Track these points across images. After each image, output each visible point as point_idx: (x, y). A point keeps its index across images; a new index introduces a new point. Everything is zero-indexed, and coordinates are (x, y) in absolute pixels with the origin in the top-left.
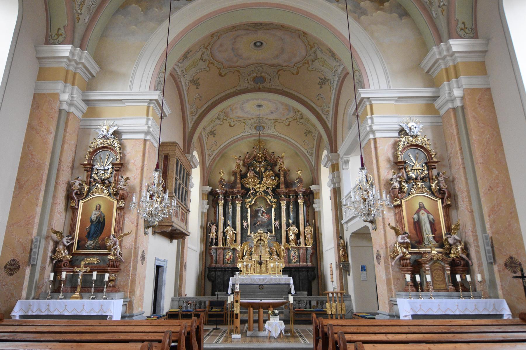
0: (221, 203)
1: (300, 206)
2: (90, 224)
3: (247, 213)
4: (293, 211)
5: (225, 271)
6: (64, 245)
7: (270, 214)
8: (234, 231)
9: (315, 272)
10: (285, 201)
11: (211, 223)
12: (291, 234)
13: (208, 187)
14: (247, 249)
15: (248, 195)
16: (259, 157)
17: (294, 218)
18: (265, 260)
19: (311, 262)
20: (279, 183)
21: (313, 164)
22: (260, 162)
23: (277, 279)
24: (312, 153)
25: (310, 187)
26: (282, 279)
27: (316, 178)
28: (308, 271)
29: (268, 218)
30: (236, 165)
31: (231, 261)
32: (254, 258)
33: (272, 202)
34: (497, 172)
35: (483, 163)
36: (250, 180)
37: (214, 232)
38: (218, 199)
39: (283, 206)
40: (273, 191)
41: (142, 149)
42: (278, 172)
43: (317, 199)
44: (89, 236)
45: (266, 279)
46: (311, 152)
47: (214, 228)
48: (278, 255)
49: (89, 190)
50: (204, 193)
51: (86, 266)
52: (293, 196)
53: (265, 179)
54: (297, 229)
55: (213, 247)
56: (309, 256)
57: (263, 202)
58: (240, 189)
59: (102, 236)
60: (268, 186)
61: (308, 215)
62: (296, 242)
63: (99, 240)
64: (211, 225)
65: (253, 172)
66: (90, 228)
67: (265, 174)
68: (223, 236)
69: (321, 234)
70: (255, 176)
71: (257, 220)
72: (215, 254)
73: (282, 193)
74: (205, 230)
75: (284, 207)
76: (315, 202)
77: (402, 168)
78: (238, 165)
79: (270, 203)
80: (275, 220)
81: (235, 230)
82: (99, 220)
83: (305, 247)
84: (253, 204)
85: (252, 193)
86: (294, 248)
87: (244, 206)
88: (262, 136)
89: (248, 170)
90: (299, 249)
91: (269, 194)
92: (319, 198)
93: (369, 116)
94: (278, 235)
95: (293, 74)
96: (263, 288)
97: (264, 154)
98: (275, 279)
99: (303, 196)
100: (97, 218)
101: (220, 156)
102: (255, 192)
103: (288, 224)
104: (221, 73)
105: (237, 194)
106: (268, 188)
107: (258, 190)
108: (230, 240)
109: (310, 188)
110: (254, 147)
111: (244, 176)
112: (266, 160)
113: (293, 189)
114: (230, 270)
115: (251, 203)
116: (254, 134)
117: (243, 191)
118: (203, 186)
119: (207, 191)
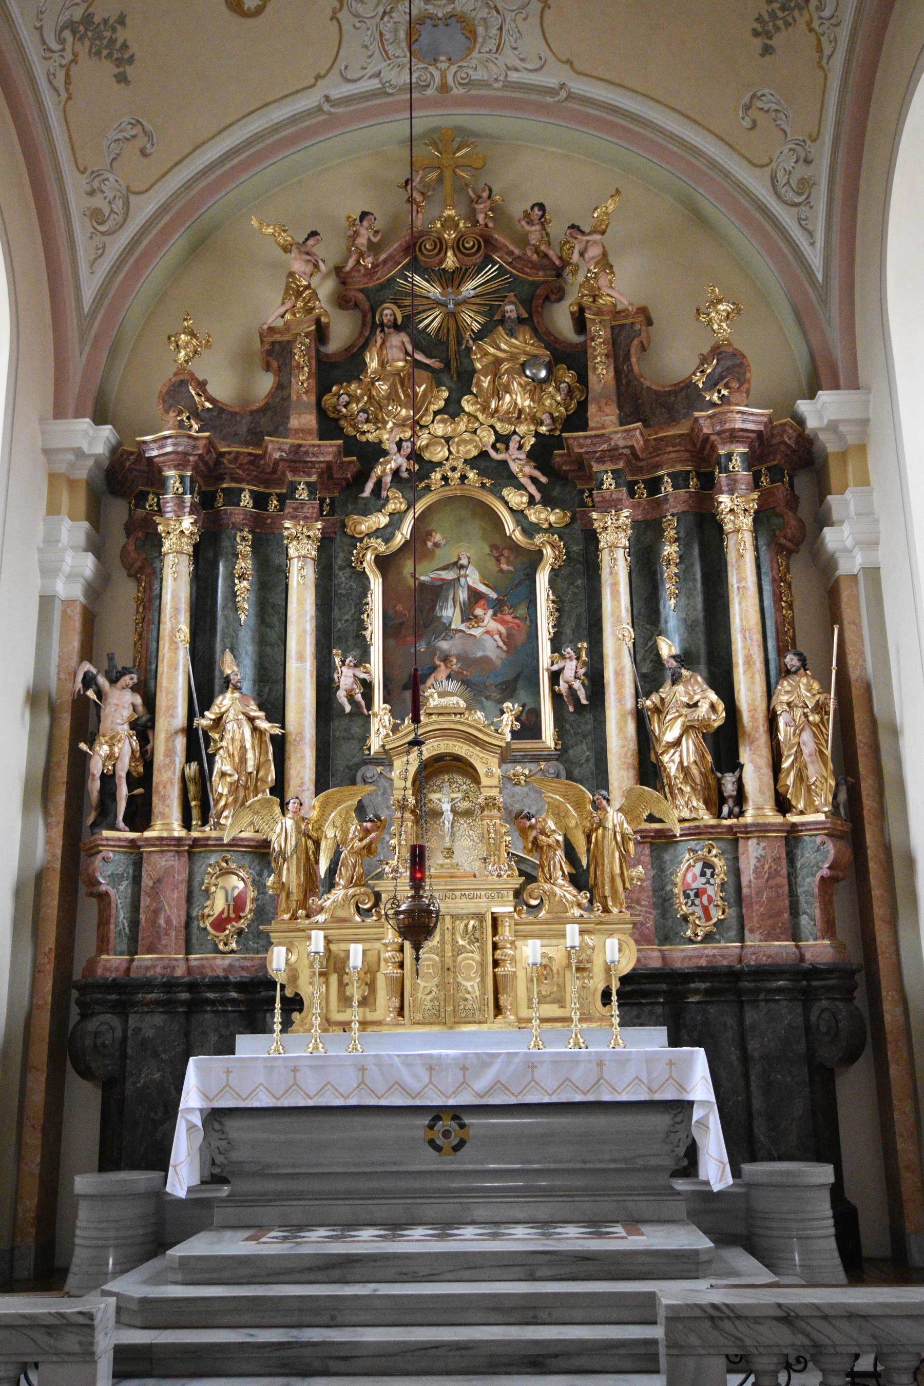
1: (731, 543)
4: (684, 578)
5: (195, 1006)
7: (522, 611)
8: (264, 725)
10: (626, 513)
11: (107, 675)
13: (85, 423)
14: (345, 833)
15: (370, 486)
16: (441, 246)
17: (690, 627)
18: (480, 917)
19: (829, 929)
20: (583, 406)
21: (816, 262)
22: (451, 279)
23: (574, 1061)
24: (805, 186)
25: (804, 406)
26: (622, 1061)
27: (839, 354)
28: (807, 997)
29: (508, 640)
31: (240, 932)
33: (530, 530)
37: (124, 729)
39: (612, 547)
42: (575, 338)
43: (848, 494)
45: (486, 1061)
46: (802, 171)
48: (578, 880)
50: (62, 468)
52: (679, 480)
54: (713, 696)
55: (106, 833)
56: (809, 884)
57: (475, 528)
61: (790, 606)
62: (715, 797)
64: (102, 680)
65: (398, 340)
68: (189, 760)
69: (895, 733)
70: (417, 364)
71: (432, 650)
73: (601, 460)
75: (620, 554)
76: (835, 515)
79: (518, 536)
80: (557, 646)
83: (779, 819)
84: (406, 543)
85: (396, 472)
86: (697, 832)
88: (461, 102)
91: (512, 480)
92: (864, 481)
96: (462, 1143)
98: (558, 1061)
101: (177, 245)
105: (290, 477)
106: (503, 440)
107: (439, 453)
108: (234, 788)
109: (800, 421)
112: (488, 260)
114: (234, 1002)
115: (387, 541)
117: (329, 450)
119: (79, 453)
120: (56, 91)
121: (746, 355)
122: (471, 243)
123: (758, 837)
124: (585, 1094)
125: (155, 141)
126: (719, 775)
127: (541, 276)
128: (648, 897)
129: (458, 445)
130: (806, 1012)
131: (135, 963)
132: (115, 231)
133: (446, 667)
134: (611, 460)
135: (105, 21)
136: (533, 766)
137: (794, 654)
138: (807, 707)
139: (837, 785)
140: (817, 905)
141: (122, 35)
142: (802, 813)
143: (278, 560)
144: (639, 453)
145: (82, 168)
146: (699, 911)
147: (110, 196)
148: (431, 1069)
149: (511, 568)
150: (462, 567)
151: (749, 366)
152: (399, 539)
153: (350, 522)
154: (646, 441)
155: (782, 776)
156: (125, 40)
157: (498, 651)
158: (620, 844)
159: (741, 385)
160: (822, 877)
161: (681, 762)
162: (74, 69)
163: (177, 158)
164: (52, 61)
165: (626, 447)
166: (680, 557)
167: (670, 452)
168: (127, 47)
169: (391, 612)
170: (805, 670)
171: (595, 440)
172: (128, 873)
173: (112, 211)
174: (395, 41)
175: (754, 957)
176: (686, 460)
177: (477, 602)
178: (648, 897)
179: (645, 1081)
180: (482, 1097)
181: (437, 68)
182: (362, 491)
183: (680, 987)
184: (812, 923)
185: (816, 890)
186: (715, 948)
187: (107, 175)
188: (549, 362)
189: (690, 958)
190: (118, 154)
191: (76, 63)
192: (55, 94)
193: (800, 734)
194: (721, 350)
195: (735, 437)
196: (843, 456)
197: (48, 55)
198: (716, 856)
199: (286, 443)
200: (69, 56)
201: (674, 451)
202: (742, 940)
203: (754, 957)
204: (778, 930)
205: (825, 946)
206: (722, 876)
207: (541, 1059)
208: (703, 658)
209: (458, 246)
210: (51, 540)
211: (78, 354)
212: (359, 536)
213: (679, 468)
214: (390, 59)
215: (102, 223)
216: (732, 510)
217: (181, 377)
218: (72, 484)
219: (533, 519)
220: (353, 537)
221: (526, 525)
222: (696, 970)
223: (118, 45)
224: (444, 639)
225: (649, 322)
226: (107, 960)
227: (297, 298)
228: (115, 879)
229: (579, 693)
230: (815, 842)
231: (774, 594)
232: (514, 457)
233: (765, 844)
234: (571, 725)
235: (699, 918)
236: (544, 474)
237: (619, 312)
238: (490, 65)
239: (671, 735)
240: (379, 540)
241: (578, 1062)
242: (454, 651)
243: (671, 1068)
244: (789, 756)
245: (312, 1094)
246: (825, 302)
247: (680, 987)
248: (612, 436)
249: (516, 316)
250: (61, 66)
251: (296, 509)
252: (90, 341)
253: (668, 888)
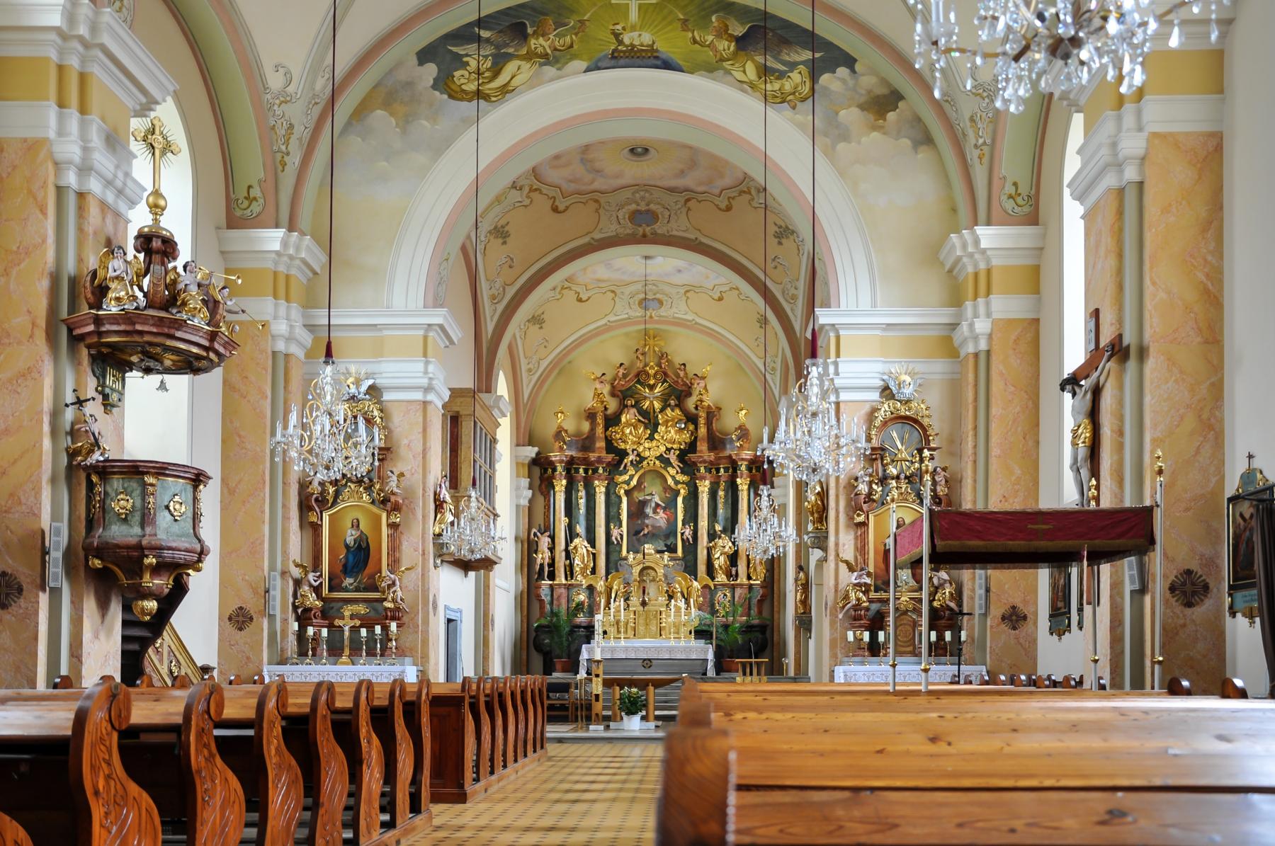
0: (560, 485)
1: (740, 494)
2: (345, 551)
3: (619, 508)
4: (725, 503)
6: (311, 586)
7: (673, 511)
8: (590, 549)
11: (539, 531)
12: (716, 556)
16: (648, 375)
17: (726, 520)
20: (696, 438)
30: (595, 395)
32: (633, 606)
33: (677, 483)
34: (1019, 472)
35: (1000, 457)
36: (628, 431)
37: (546, 550)
38: (553, 477)
40: (682, 456)
41: (421, 419)
42: (694, 411)
44: (347, 571)
46: (772, 364)
47: (545, 542)
49: (337, 494)
50: (521, 461)
51: (352, 617)
52: (726, 470)
53: (661, 429)
55: (543, 582)
56: (754, 601)
57: (658, 481)
58: (604, 454)
59: (368, 571)
60: (669, 446)
63: (364, 578)
64: (538, 534)
65: (634, 411)
66: (346, 557)
67: (663, 417)
68: (566, 559)
70: (639, 421)
72: (549, 598)
73: (700, 463)
74: (526, 546)
77: (876, 459)
78: (598, 395)
81: (593, 546)
82: (360, 544)
85: (632, 462)
86: (724, 585)
87: (612, 491)
89: (623, 407)
90: (733, 588)
91: (670, 464)
93: (832, 359)
94: (690, 557)
95: (720, 209)
97: (661, 367)
99: (749, 469)
100: (355, 540)
102: (638, 459)
103: (711, 532)
104: (557, 206)
106: (668, 450)
107: (647, 454)
108: (581, 568)
110: (637, 350)
111: (612, 421)
112: (665, 381)
113: (727, 453)
115: (628, 484)
117: (610, 457)
118: (518, 445)
119: (527, 456)
127: (684, 388)
143: (593, 492)
228: (546, 595)
239: (716, 556)
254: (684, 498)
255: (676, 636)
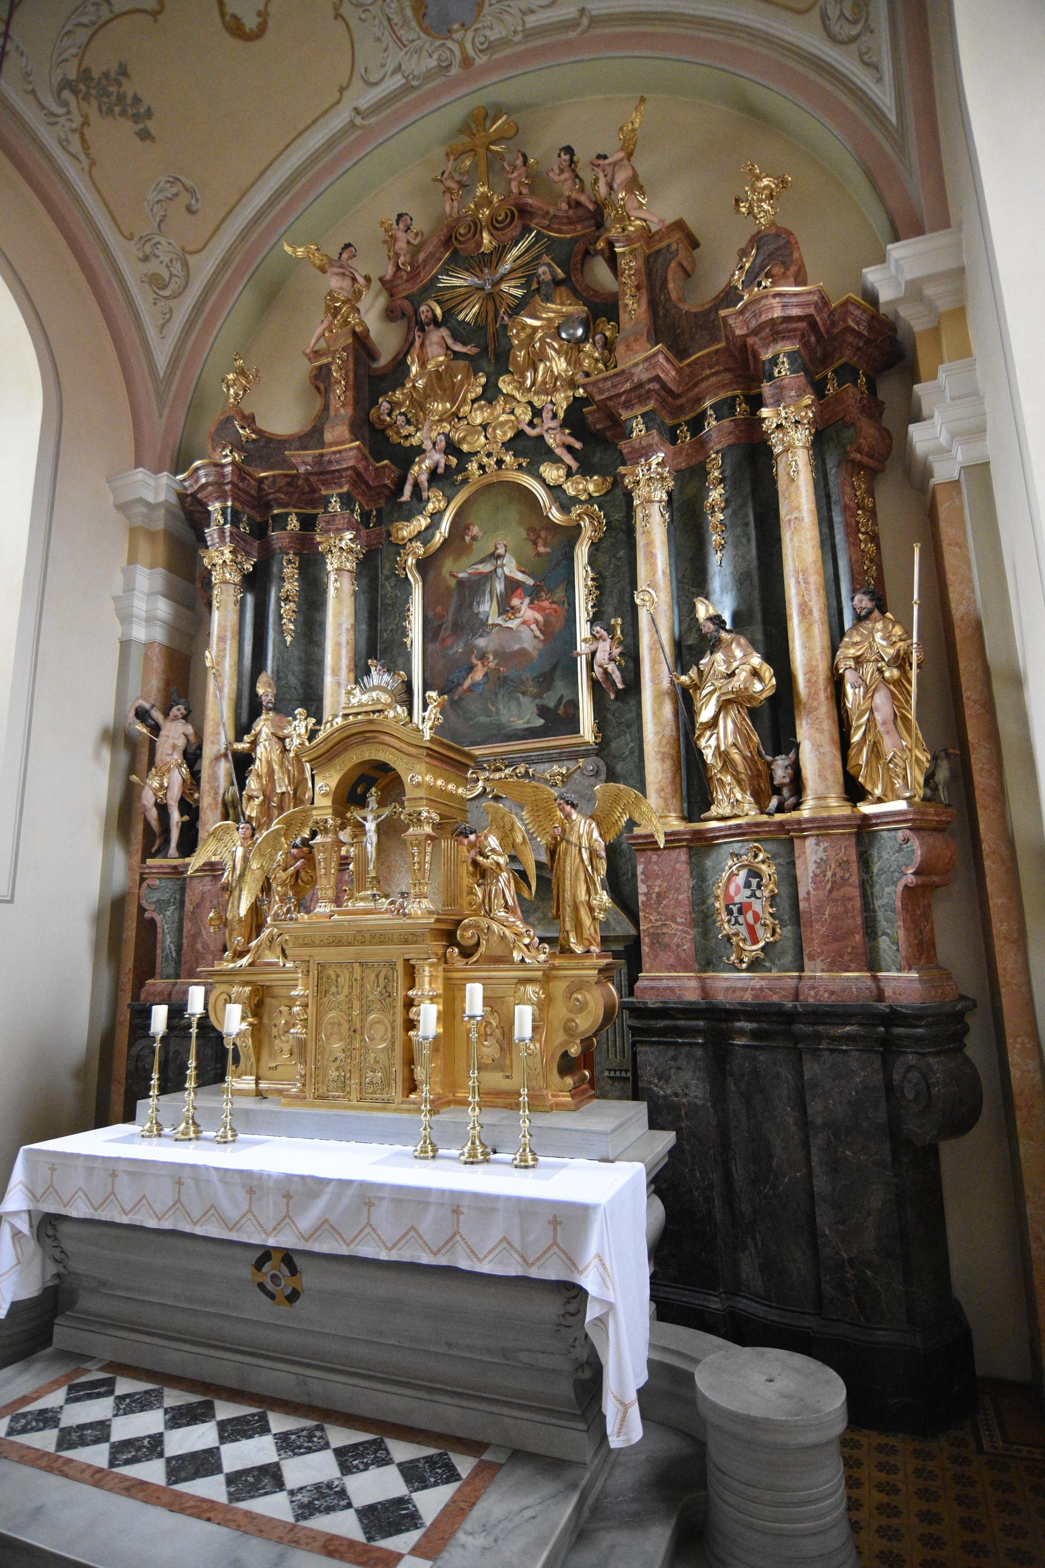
7: (560, 594)
9: (969, 1051)
12: (705, 715)
21: (884, 97)
25: (872, 275)
29: (545, 628)
50: (139, 522)
52: (724, 409)
54: (756, 660)
57: (512, 513)
61: (874, 538)
69: (1017, 681)
70: (457, 355)
71: (470, 649)
73: (628, 405)
79: (556, 515)
83: (847, 811)
84: (445, 540)
92: (964, 351)
102: (454, 461)
109: (871, 297)
112: (526, 230)
116: (428, 76)
119: (151, 507)
120: (74, 156)
121: (793, 232)
122: (503, 215)
123: (817, 835)
124: (435, 1254)
125: (199, 196)
126: (769, 758)
128: (684, 913)
129: (494, 429)
130: (887, 1067)
131: (176, 988)
132: (180, 294)
133: (483, 665)
134: (640, 402)
135: (106, 75)
136: (573, 765)
137: (864, 593)
138: (883, 660)
139: (935, 759)
140: (900, 923)
141: (129, 88)
142: (880, 800)
144: (674, 388)
145: (128, 235)
146: (743, 931)
147: (167, 260)
148: (251, 1192)
149: (548, 550)
150: (499, 557)
151: (796, 243)
152: (438, 538)
153: (393, 531)
154: (679, 371)
155: (853, 752)
156: (135, 95)
157: (536, 641)
158: (587, 862)
159: (787, 269)
160: (906, 886)
161: (718, 747)
162: (86, 130)
163: (227, 209)
164: (59, 126)
165: (650, 380)
166: (726, 501)
167: (707, 377)
168: (140, 100)
169: (430, 614)
170: (883, 612)
171: (615, 380)
172: (175, 899)
173: (172, 275)
174: (405, 23)
175: (812, 993)
176: (731, 383)
177: (513, 592)
178: (684, 913)
179: (517, 1245)
180: (307, 1240)
181: (453, 40)
182: (401, 493)
183: (724, 1026)
184: (895, 948)
185: (899, 904)
186: (762, 978)
187: (157, 239)
188: (587, 318)
189: (734, 990)
190: (164, 216)
191: (89, 125)
192: (75, 161)
193: (872, 696)
194: (762, 234)
195: (777, 333)
196: (935, 332)
197: (53, 120)
198: (763, 862)
199: (307, 455)
200: (78, 120)
201: (713, 375)
202: (801, 969)
203: (812, 993)
204: (846, 958)
205: (911, 980)
206: (771, 886)
207: (380, 1195)
208: (758, 616)
209: (494, 225)
210: (129, 588)
211: (157, 414)
212: (401, 543)
213: (723, 395)
214: (405, 46)
215: (164, 287)
216: (779, 426)
217: (227, 415)
218: (151, 535)
219: (571, 492)
220: (398, 545)
221: (564, 501)
222: (738, 1007)
223: (129, 101)
224: (481, 636)
225: (694, 244)
226: (153, 985)
227: (335, 316)
228: (161, 906)
229: (614, 676)
230: (895, 839)
231: (847, 525)
232: (546, 427)
233: (826, 844)
234: (613, 715)
235: (744, 940)
236: (578, 439)
237: (653, 236)
238: (505, 16)
240: (418, 544)
241: (428, 1204)
242: (491, 648)
243: (555, 1230)
244: (859, 727)
245: (127, 1208)
246: (901, 147)
247: (724, 1026)
248: (633, 371)
249: (550, 277)
250: (73, 131)
251: (328, 522)
252: (169, 404)
253: (711, 901)
254: (595, 547)
255: (495, 1080)
